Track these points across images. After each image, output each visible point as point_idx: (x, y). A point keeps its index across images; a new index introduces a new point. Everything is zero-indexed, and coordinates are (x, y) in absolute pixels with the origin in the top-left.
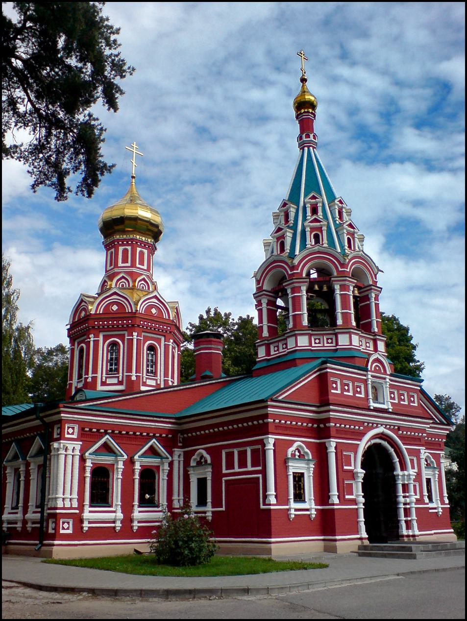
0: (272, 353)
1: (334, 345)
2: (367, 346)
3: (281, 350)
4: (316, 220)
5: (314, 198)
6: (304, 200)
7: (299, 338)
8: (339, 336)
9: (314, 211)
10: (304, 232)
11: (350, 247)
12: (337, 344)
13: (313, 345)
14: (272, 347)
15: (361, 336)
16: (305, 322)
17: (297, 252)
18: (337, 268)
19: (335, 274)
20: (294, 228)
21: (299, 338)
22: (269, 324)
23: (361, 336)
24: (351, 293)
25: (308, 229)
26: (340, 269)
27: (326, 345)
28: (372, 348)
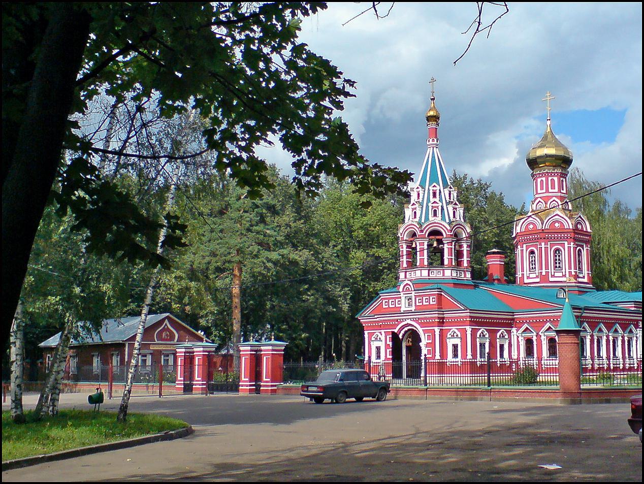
0: (407, 277)
1: (442, 275)
2: (460, 275)
3: (412, 276)
4: (435, 202)
5: (434, 186)
6: (429, 189)
7: (422, 271)
8: (445, 270)
9: (434, 196)
10: (427, 206)
11: (454, 217)
12: (443, 275)
13: (430, 275)
14: (408, 273)
15: (456, 270)
16: (426, 263)
17: (423, 221)
18: (446, 233)
19: (445, 236)
20: (421, 205)
21: (422, 271)
22: (407, 260)
23: (456, 270)
24: (453, 247)
25: (430, 208)
26: (448, 233)
27: (437, 275)
28: (463, 276)
